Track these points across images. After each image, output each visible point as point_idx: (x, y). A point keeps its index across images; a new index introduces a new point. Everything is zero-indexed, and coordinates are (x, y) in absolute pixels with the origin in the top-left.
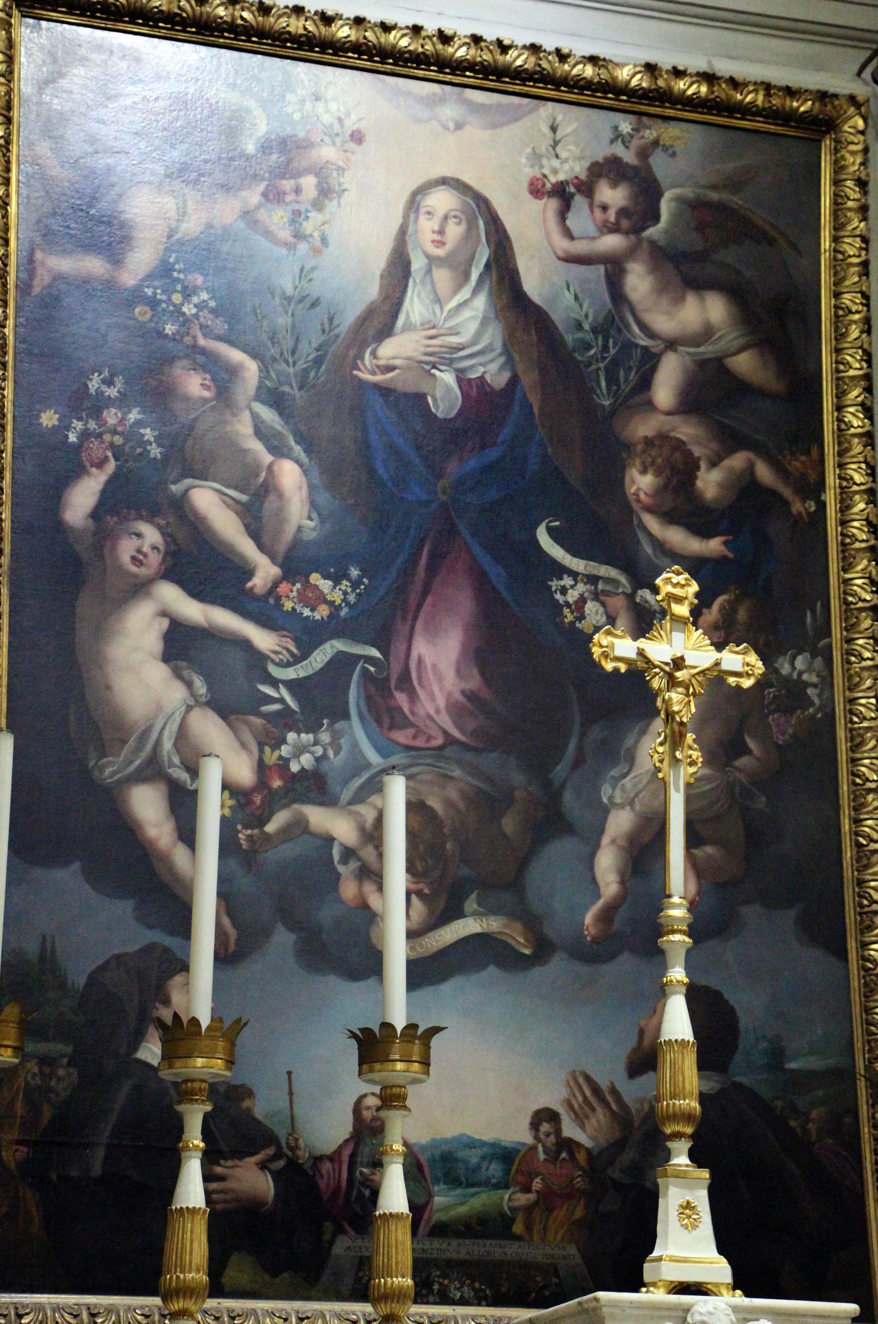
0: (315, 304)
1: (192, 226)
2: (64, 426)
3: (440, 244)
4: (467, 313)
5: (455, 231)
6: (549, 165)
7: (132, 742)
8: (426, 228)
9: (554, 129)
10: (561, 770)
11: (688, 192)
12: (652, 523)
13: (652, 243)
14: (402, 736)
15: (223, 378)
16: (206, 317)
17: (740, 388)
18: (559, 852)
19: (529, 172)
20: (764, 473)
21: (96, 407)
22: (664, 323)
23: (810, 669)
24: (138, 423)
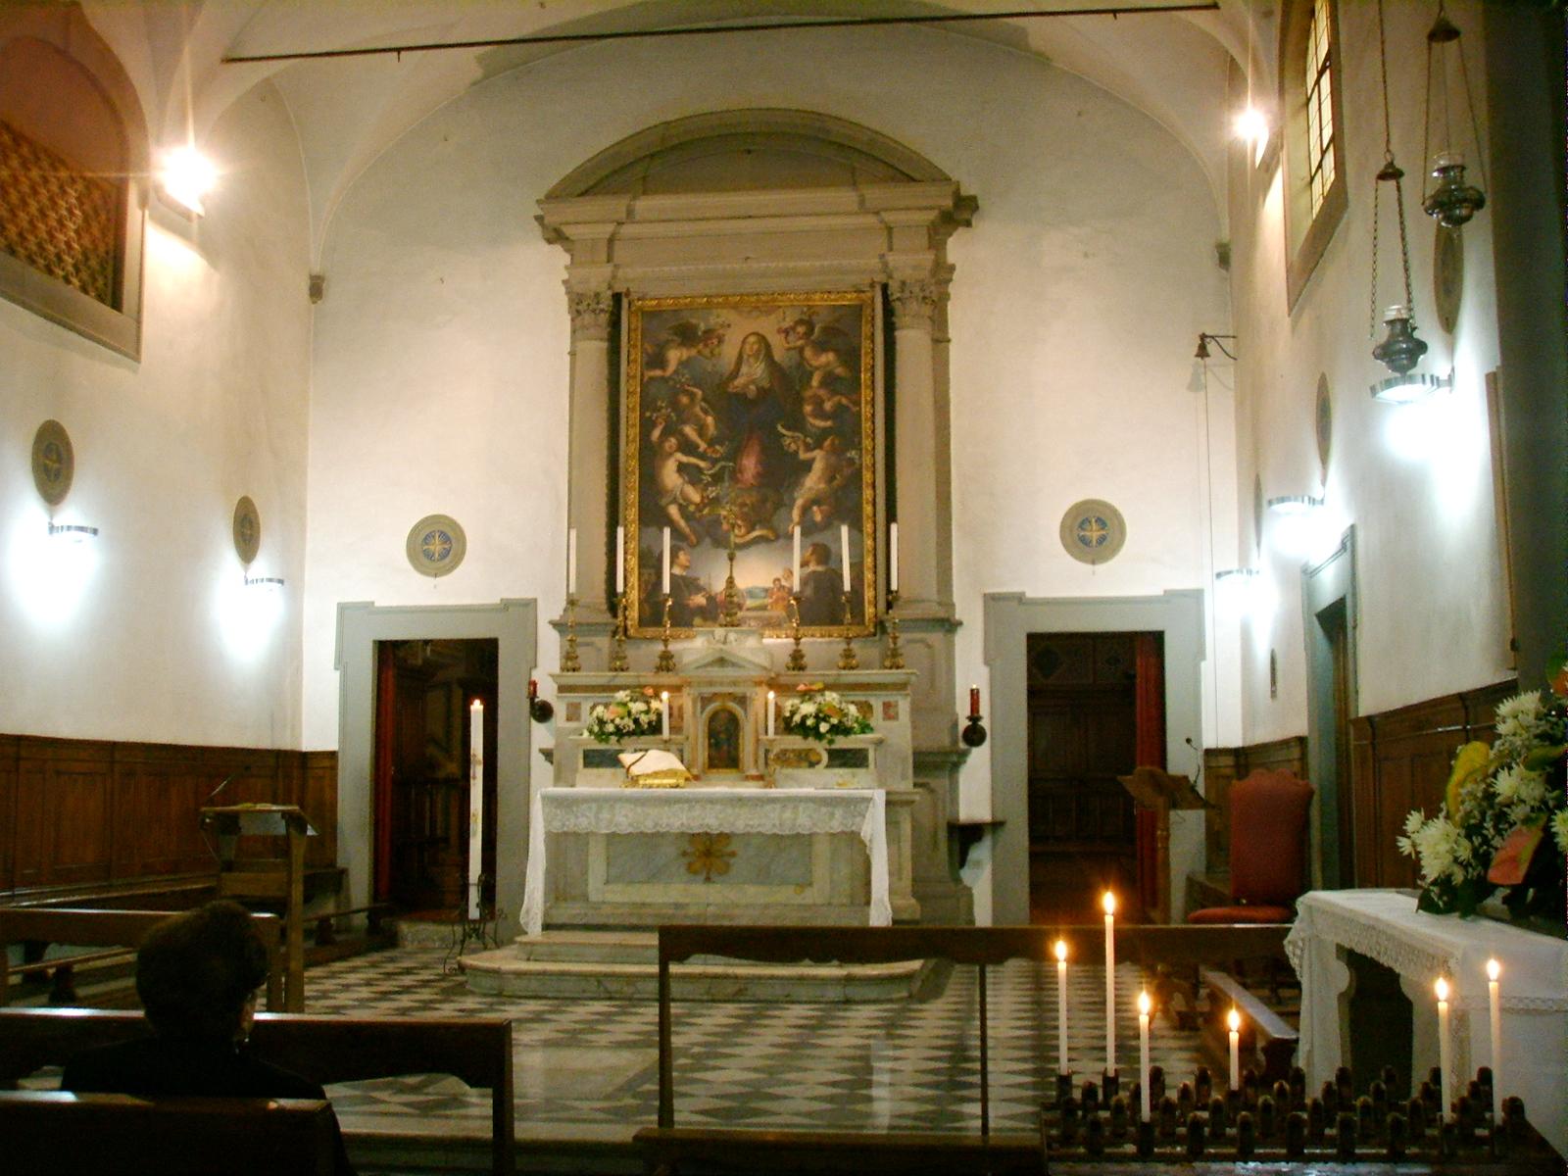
1: (685, 357)
5: (756, 347)
8: (747, 347)
12: (811, 420)
13: (813, 342)
14: (739, 485)
15: (692, 396)
17: (838, 378)
18: (783, 511)
19: (777, 327)
20: (844, 401)
22: (814, 363)
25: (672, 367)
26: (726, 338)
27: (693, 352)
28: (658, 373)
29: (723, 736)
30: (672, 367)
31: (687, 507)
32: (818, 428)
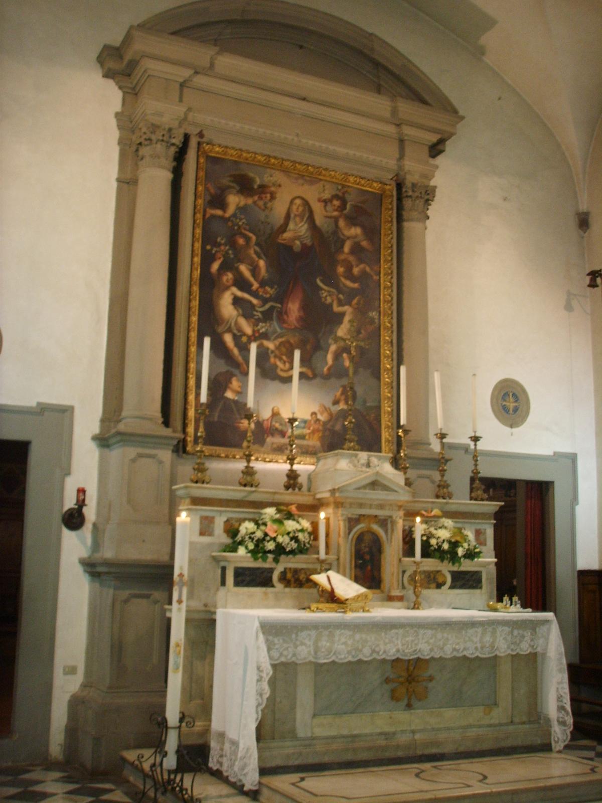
0: (269, 224)
1: (242, 204)
2: (211, 250)
3: (297, 211)
4: (303, 228)
5: (301, 209)
6: (322, 195)
7: (225, 324)
8: (294, 207)
9: (324, 186)
10: (320, 335)
11: (353, 203)
12: (343, 280)
14: (285, 325)
15: (248, 239)
16: (244, 226)
18: (319, 354)
20: (368, 269)
21: (219, 245)
23: (376, 315)
24: (229, 250)
25: (231, 210)
26: (278, 195)
27: (250, 201)
28: (219, 212)
29: (368, 557)
30: (231, 210)
31: (241, 336)
32: (348, 288)
